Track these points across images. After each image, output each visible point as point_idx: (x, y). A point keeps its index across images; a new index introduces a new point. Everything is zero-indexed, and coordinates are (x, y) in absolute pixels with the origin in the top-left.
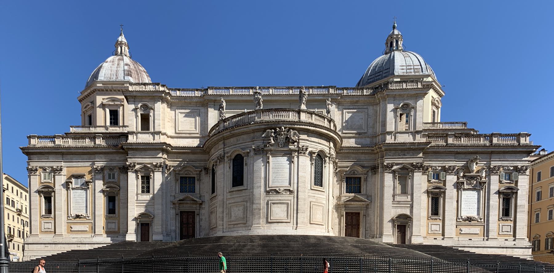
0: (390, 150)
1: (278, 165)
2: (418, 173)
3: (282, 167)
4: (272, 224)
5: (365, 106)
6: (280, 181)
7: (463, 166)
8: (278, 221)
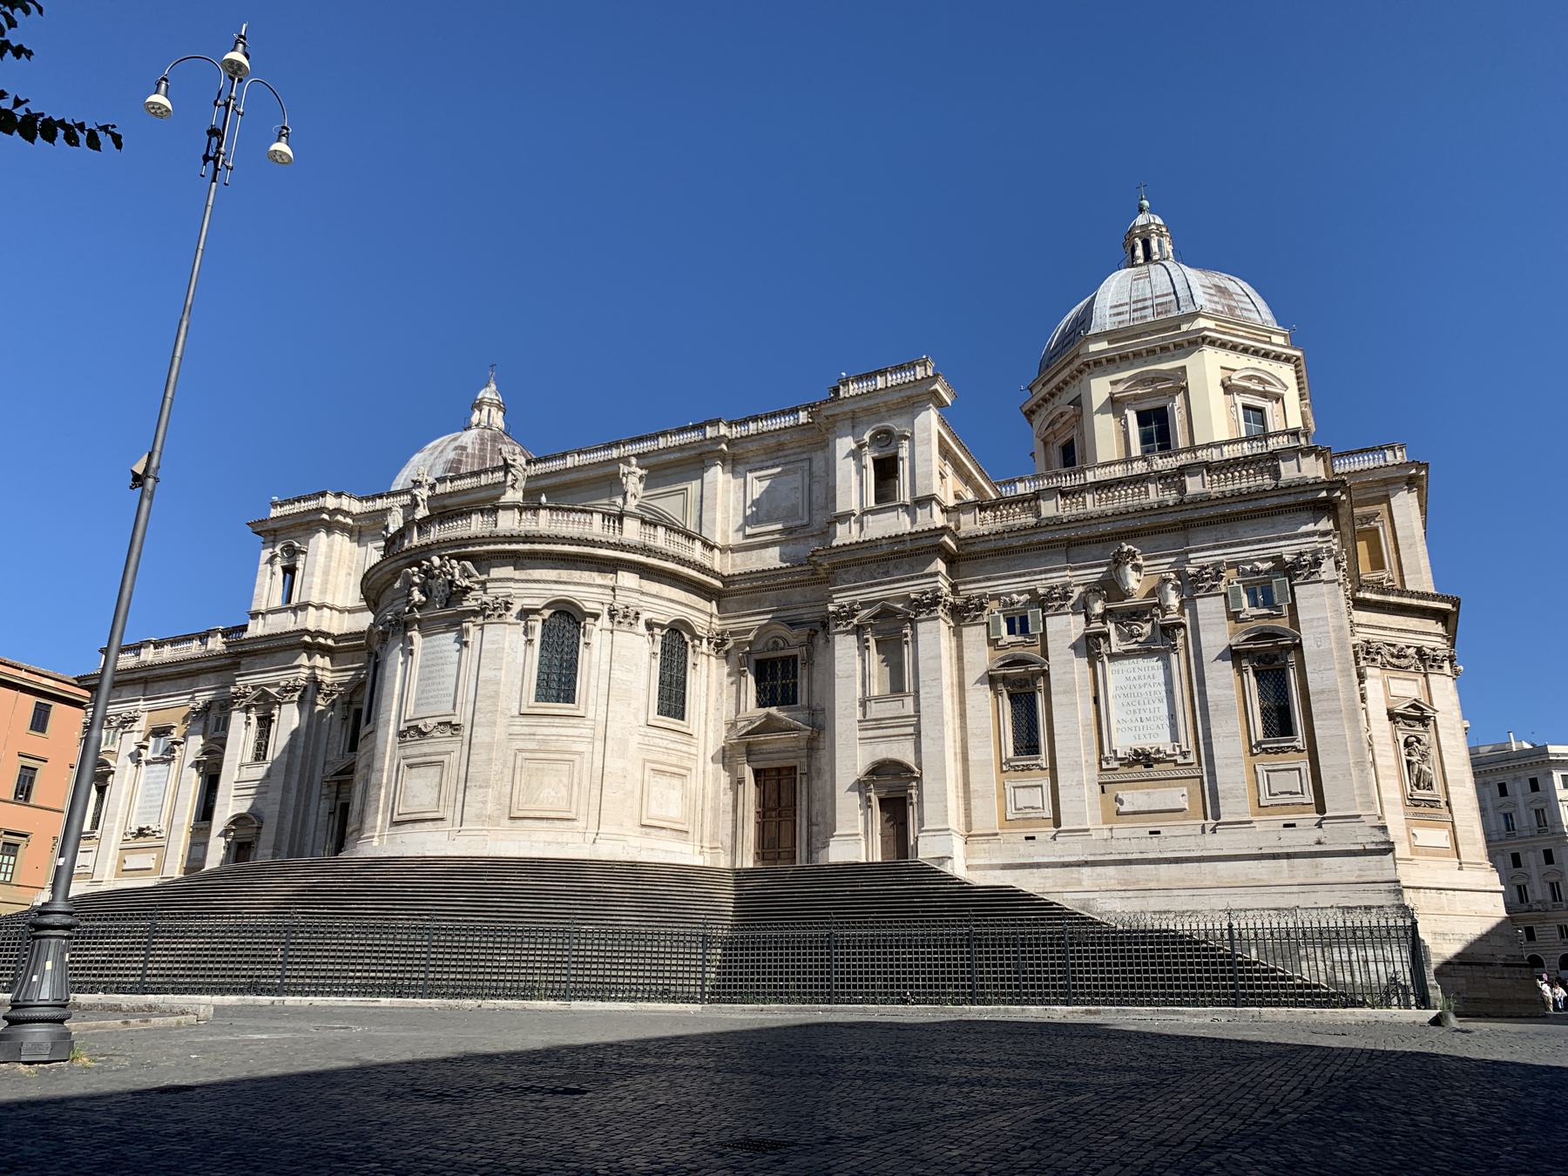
0: (844, 565)
1: (433, 656)
2: (929, 623)
3: (440, 661)
4: (401, 827)
5: (804, 453)
6: (431, 700)
7: (1099, 582)
8: (413, 817)
